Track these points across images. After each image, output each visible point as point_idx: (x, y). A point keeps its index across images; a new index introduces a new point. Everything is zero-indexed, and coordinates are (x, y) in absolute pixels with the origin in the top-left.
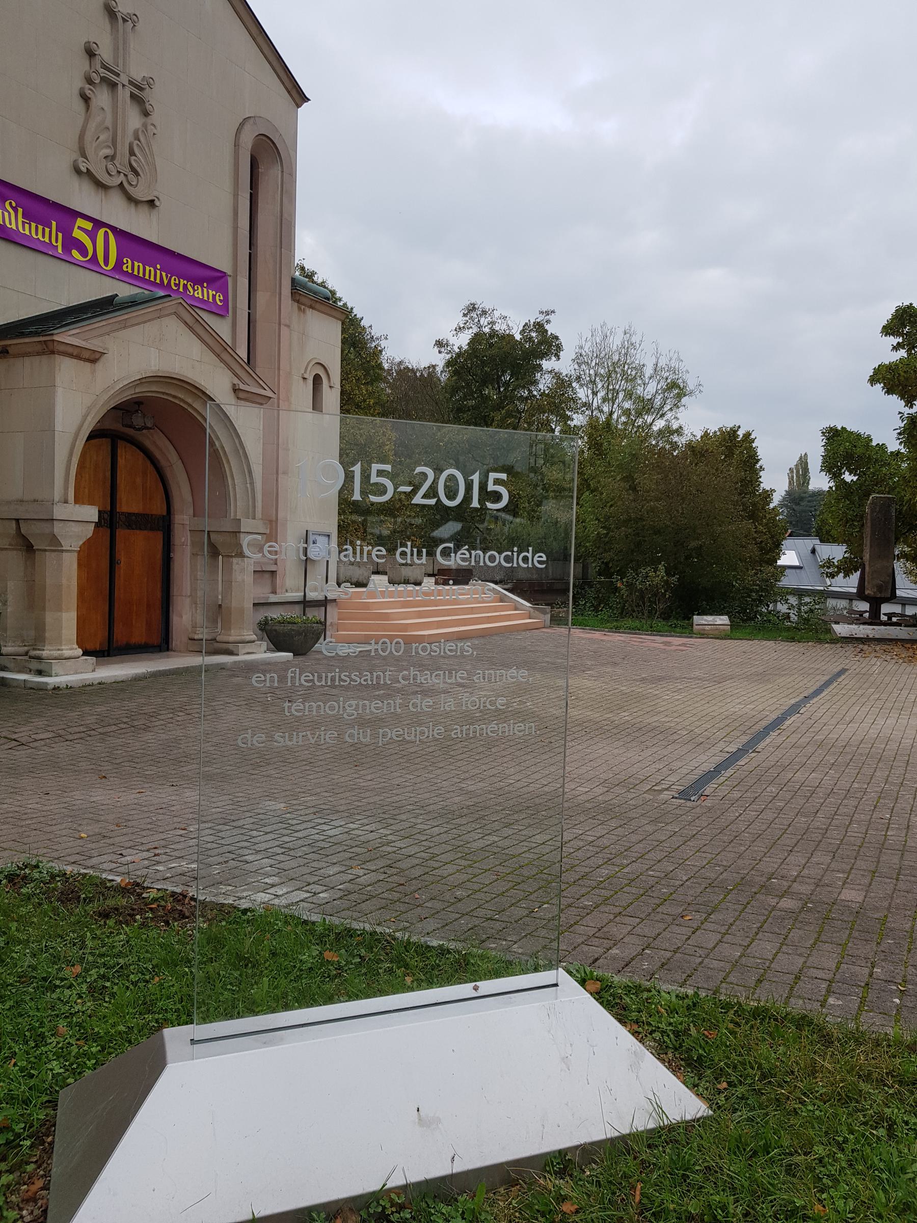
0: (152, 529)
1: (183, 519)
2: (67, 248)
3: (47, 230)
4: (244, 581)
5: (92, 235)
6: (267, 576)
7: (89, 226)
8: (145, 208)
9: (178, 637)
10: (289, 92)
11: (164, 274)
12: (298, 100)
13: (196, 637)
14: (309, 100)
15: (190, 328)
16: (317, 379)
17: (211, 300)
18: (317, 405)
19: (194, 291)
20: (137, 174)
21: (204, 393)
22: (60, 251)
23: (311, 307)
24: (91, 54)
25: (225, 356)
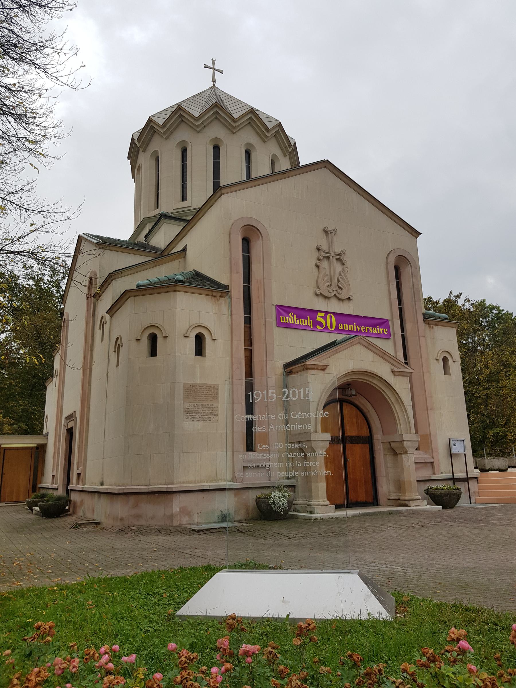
0: (363, 443)
1: (378, 437)
2: (314, 326)
3: (306, 320)
4: (409, 466)
5: (325, 318)
6: (429, 465)
7: (323, 315)
8: (346, 302)
9: (382, 499)
10: (411, 233)
11: (358, 326)
12: (416, 235)
13: (391, 498)
14: (421, 233)
15: (367, 347)
16: (445, 360)
17: (381, 333)
18: (446, 371)
19: (373, 330)
20: (341, 289)
21: (377, 375)
22: (312, 327)
24: (319, 249)
25: (385, 357)
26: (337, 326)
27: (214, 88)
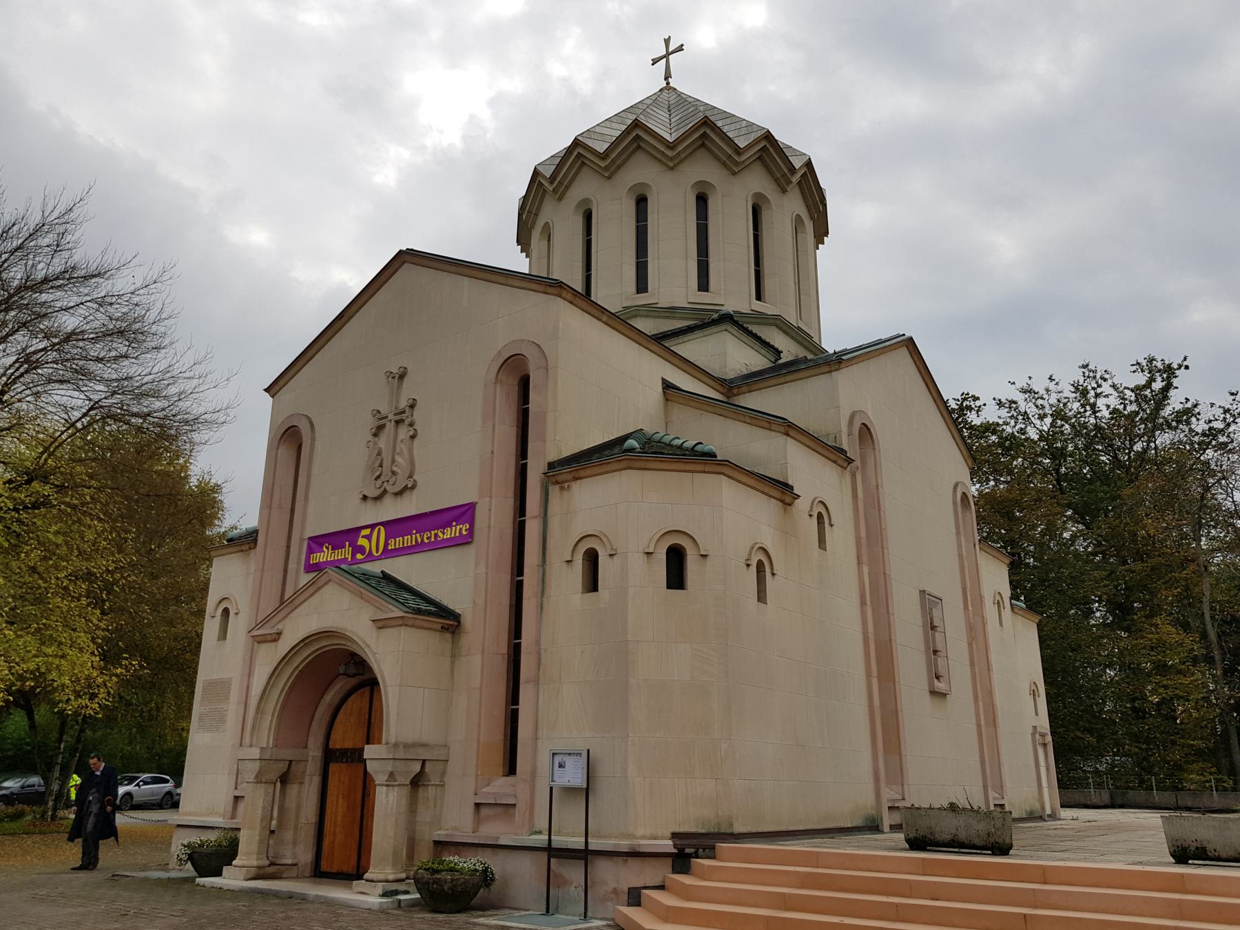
2: (353, 555)
5: (369, 537)
23: (576, 479)
26: (386, 544)
27: (668, 87)
